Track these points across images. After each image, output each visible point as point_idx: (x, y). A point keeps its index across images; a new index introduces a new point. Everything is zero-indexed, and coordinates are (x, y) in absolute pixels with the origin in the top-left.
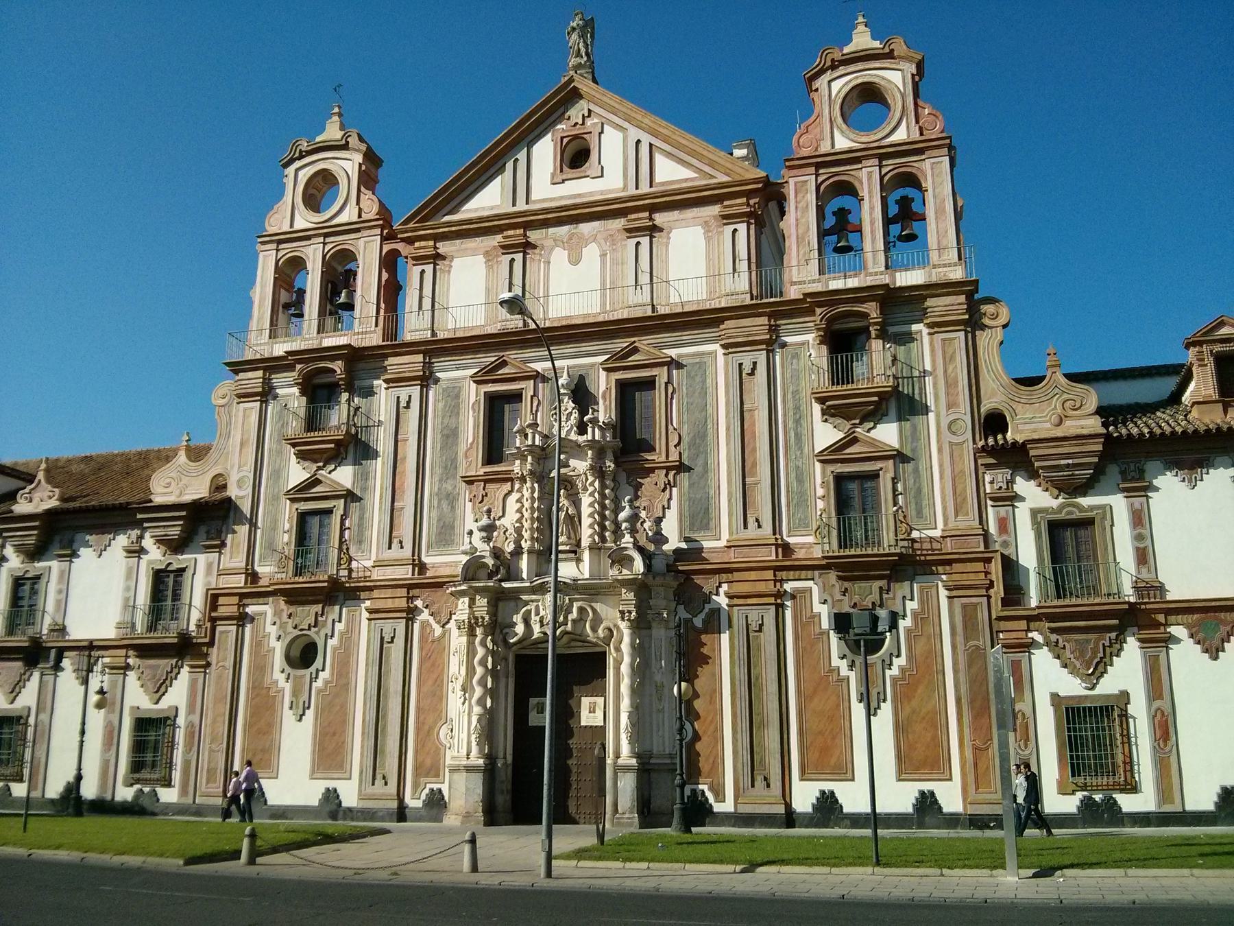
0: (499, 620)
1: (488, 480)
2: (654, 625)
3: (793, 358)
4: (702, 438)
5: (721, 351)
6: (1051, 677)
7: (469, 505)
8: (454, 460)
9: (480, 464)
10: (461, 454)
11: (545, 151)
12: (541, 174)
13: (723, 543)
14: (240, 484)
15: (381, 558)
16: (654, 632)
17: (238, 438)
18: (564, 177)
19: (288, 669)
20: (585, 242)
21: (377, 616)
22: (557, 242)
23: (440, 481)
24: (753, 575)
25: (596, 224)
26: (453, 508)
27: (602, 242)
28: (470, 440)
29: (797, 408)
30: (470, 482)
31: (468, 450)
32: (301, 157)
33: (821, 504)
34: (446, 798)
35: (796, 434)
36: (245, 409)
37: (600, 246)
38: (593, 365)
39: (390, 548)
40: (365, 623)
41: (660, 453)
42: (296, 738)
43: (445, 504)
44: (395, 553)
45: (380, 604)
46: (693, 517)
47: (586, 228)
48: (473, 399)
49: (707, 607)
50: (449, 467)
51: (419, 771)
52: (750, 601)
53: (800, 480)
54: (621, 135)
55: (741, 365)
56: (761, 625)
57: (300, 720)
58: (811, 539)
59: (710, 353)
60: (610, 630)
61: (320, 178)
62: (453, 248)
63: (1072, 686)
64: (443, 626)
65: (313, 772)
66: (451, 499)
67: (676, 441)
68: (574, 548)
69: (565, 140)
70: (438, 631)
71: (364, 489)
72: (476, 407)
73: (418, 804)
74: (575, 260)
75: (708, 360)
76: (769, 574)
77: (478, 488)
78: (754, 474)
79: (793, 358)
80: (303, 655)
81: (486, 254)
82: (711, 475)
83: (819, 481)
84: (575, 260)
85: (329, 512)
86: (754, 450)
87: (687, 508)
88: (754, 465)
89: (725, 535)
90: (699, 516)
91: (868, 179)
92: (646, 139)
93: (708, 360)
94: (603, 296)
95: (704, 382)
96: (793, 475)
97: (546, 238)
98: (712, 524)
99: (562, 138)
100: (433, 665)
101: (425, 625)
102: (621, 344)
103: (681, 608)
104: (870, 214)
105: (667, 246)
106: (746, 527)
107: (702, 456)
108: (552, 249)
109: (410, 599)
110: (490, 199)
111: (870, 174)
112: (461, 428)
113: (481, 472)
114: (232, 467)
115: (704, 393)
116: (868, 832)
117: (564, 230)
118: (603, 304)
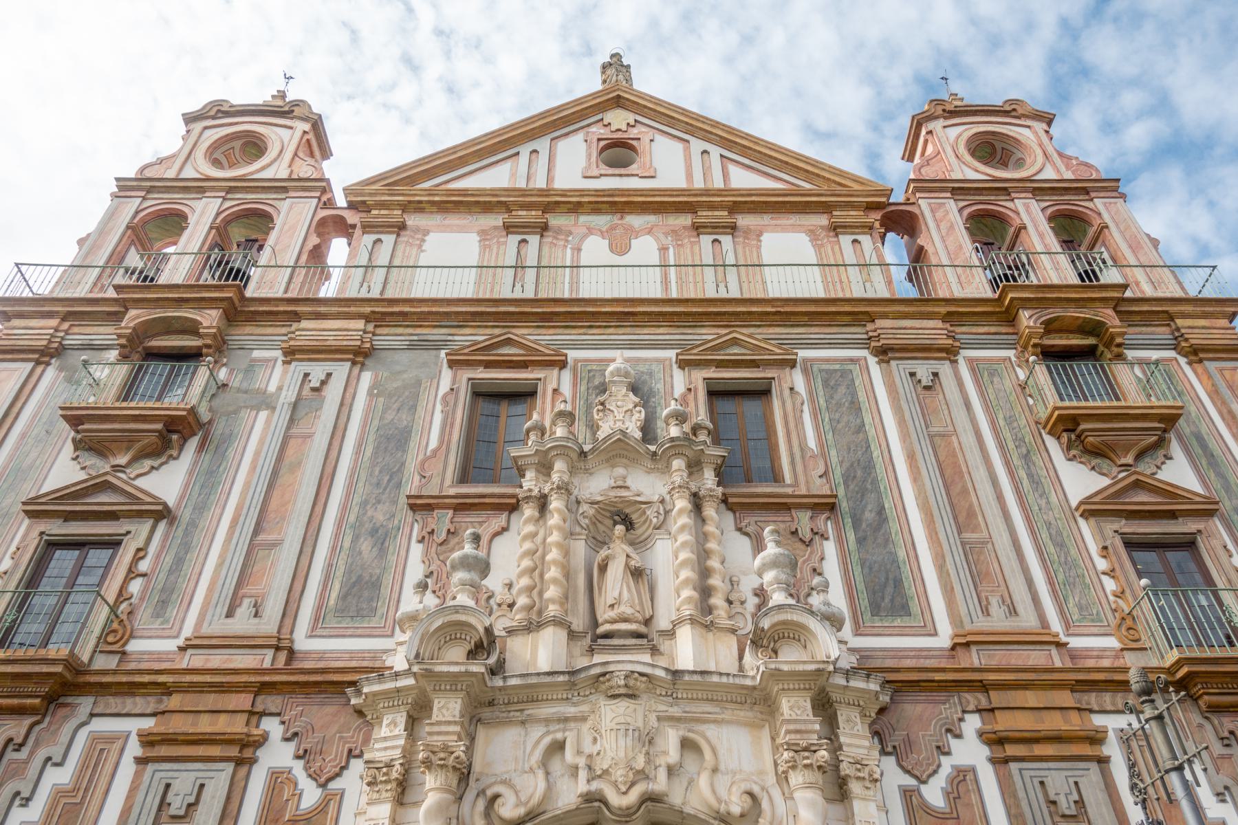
0: (477, 767)
1: (463, 506)
2: (855, 787)
3: (991, 375)
5: (872, 361)
7: (417, 550)
9: (448, 482)
10: (412, 464)
13: (943, 640)
15: (206, 630)
16: (857, 805)
18: (603, 172)
20: (634, 233)
21: (164, 751)
22: (590, 231)
23: (364, 504)
24: (1031, 698)
25: (651, 219)
26: (382, 552)
27: (661, 236)
28: (433, 443)
29: (1019, 441)
30: (421, 506)
31: (423, 463)
32: (214, 118)
33: (1110, 585)
35: (1030, 476)
37: (657, 239)
38: (658, 361)
39: (229, 614)
40: (127, 769)
41: (796, 484)
43: (366, 546)
44: (242, 623)
45: (179, 725)
47: (636, 221)
48: (445, 386)
49: (947, 764)
52: (1038, 750)
53: (1060, 545)
54: (679, 146)
55: (912, 375)
56: (1080, 803)
58: (1112, 643)
59: (852, 360)
60: (751, 794)
61: (237, 144)
62: (430, 223)
64: (323, 786)
66: (382, 538)
67: (821, 470)
68: (643, 629)
69: (602, 143)
70: (311, 795)
71: (201, 508)
72: (451, 399)
74: (620, 248)
75: (856, 369)
76: (1065, 698)
77: (443, 520)
78: (975, 529)
79: (991, 375)
81: (483, 233)
82: (894, 526)
83: (1093, 548)
84: (620, 248)
85: (113, 544)
86: (965, 491)
87: (859, 578)
88: (971, 514)
90: (885, 594)
92: (715, 151)
93: (856, 369)
95: (854, 394)
96: (1045, 535)
97: (576, 224)
98: (915, 607)
99: (599, 140)
101: (279, 780)
102: (708, 334)
103: (890, 762)
105: (759, 247)
106: (986, 612)
107: (872, 496)
108: (585, 237)
109: (255, 715)
111: (1027, 207)
112: (417, 428)
113: (452, 492)
115: (855, 407)
117: (602, 221)
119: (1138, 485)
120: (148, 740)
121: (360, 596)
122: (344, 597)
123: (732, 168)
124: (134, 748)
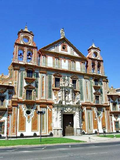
4: (81, 89)
6: (114, 119)
7: (53, 93)
8: (51, 86)
10: (52, 85)
11: (60, 47)
12: (59, 49)
14: (15, 83)
17: (14, 76)
19: (27, 114)
26: (51, 93)
30: (53, 90)
34: (53, 133)
36: (16, 71)
42: (29, 126)
46: (81, 98)
50: (50, 87)
51: (49, 130)
57: (29, 123)
63: (115, 120)
65: (32, 130)
70: (51, 110)
73: (49, 134)
74: (65, 62)
77: (55, 91)
80: (28, 112)
84: (65, 62)
89: (85, 101)
90: (82, 98)
91: (96, 63)
94: (68, 68)
100: (50, 115)
104: (96, 66)
110: (53, 50)
114: (13, 81)
116: (40, 138)
118: (68, 69)
119: (97, 92)
120: (40, 106)
121: (50, 96)
122: (49, 96)
123: (74, 52)
124: (39, 107)
